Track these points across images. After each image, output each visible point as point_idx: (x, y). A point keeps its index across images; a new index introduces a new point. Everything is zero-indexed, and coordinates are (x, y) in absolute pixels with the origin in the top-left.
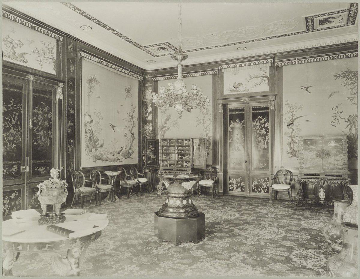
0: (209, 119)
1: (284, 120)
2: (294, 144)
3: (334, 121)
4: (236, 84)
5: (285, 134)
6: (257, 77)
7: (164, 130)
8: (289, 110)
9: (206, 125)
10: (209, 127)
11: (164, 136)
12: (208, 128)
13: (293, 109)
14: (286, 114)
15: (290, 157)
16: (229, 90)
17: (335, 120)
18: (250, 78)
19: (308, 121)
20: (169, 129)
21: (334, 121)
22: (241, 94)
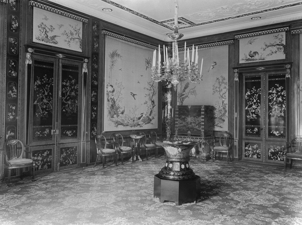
0: (225, 88)
9: (221, 93)
10: (225, 95)
16: (245, 59)
20: (187, 96)
22: (257, 62)
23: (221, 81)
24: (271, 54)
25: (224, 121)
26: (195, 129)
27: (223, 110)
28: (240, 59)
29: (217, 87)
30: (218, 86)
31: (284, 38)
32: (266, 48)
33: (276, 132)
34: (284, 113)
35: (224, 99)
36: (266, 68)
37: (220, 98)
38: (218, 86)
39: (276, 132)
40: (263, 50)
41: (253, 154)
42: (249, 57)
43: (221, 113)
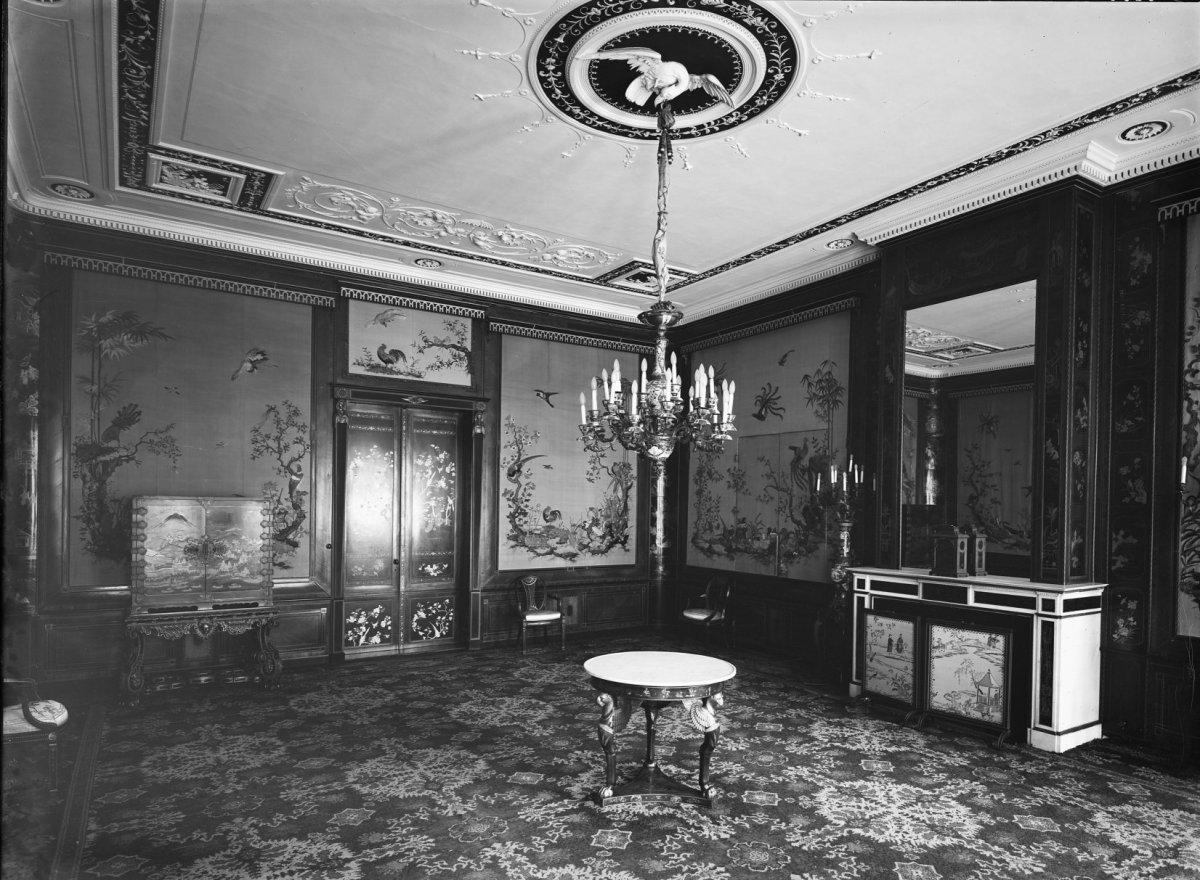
0: (300, 441)
1: (501, 463)
2: (521, 517)
3: (591, 471)
4: (387, 351)
5: (504, 494)
6: (444, 346)
7: (106, 464)
8: (512, 440)
9: (286, 458)
10: (298, 462)
11: (102, 483)
12: (294, 467)
13: (521, 437)
14: (505, 447)
15: (512, 547)
17: (593, 469)
18: (423, 344)
19: (547, 467)
20: (129, 459)
21: (591, 471)
23: (283, 416)
24: (439, 367)
25: (295, 545)
26: (234, 582)
27: (291, 511)
28: (351, 360)
29: (268, 437)
30: (275, 433)
31: (469, 335)
32: (424, 347)
33: (432, 567)
34: (451, 518)
35: (294, 478)
36: (430, 402)
37: (282, 474)
38: (275, 433)
39: (432, 567)
40: (416, 349)
41: (372, 633)
42: (377, 360)
43: (284, 521)
